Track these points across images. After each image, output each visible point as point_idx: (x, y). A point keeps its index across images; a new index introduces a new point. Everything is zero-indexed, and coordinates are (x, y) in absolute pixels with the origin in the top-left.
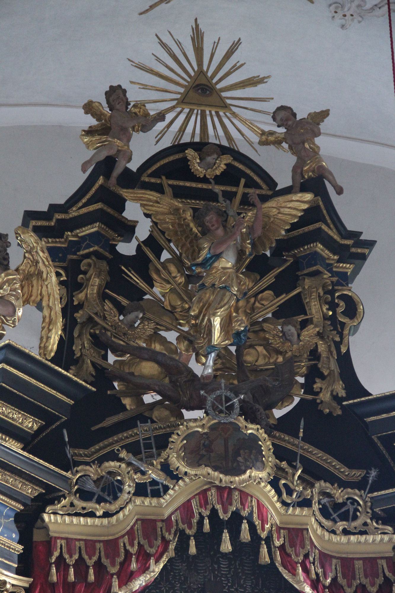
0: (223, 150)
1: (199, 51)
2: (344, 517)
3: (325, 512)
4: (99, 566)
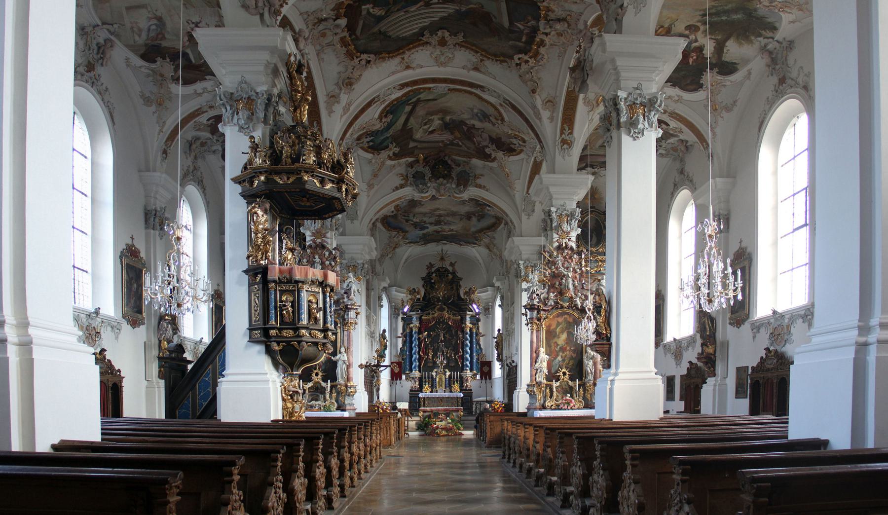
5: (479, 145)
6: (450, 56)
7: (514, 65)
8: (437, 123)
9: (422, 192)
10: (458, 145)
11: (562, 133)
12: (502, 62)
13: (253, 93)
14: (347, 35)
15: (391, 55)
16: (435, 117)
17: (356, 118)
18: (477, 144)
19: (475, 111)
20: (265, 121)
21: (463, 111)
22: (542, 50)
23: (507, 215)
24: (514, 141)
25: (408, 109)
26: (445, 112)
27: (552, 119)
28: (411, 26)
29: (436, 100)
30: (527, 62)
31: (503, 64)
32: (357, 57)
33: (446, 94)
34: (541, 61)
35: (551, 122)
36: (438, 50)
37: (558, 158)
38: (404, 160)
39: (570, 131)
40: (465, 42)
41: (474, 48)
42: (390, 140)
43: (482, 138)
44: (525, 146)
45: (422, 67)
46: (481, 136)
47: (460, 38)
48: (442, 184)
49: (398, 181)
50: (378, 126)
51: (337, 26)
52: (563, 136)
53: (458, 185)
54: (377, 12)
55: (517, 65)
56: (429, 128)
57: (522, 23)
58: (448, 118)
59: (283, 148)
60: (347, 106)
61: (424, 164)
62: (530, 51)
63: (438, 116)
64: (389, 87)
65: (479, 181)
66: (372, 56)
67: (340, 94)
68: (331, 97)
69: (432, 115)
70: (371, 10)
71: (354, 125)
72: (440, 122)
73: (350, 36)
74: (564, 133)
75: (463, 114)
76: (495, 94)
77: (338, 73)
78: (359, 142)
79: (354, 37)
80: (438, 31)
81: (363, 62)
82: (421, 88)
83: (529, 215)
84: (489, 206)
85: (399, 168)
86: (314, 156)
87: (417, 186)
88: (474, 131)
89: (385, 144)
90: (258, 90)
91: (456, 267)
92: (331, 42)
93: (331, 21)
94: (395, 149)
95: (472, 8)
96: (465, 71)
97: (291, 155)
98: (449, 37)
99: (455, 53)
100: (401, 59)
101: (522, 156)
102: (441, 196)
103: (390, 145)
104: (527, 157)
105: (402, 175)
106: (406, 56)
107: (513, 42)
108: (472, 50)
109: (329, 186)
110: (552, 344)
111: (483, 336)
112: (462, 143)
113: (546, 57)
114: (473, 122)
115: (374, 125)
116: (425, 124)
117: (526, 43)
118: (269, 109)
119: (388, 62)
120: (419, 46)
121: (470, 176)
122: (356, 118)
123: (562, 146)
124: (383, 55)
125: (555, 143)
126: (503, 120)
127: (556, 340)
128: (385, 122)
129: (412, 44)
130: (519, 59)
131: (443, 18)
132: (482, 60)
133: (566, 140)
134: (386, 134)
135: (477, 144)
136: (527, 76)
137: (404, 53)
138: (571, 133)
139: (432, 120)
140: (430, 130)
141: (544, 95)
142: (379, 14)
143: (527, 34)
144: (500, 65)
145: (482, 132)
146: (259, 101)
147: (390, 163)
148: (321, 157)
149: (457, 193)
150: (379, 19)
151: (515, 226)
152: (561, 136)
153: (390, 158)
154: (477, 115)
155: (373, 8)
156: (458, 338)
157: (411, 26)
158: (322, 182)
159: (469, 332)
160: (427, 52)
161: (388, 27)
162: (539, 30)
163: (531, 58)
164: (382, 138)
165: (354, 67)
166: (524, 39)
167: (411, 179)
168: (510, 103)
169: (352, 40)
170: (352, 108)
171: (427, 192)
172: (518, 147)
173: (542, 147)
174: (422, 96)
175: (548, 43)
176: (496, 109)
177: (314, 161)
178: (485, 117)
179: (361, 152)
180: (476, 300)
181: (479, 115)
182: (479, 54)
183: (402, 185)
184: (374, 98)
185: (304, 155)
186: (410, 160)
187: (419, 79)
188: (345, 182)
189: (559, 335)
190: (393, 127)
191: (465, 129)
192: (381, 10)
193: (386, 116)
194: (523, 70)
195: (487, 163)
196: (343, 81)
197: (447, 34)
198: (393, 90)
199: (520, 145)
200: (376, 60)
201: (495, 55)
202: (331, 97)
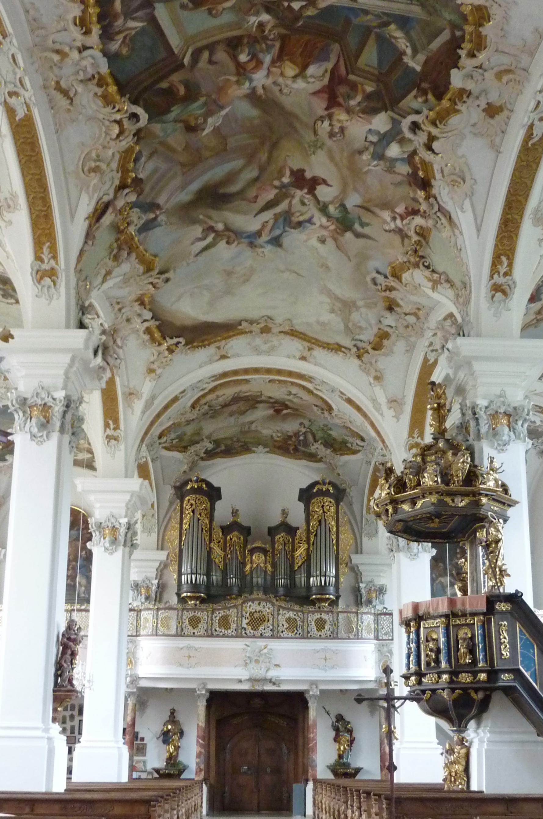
57: (133, 32)
70: (409, 51)
79: (458, 33)
143: (116, 17)
155: (404, 53)
192: (396, 38)
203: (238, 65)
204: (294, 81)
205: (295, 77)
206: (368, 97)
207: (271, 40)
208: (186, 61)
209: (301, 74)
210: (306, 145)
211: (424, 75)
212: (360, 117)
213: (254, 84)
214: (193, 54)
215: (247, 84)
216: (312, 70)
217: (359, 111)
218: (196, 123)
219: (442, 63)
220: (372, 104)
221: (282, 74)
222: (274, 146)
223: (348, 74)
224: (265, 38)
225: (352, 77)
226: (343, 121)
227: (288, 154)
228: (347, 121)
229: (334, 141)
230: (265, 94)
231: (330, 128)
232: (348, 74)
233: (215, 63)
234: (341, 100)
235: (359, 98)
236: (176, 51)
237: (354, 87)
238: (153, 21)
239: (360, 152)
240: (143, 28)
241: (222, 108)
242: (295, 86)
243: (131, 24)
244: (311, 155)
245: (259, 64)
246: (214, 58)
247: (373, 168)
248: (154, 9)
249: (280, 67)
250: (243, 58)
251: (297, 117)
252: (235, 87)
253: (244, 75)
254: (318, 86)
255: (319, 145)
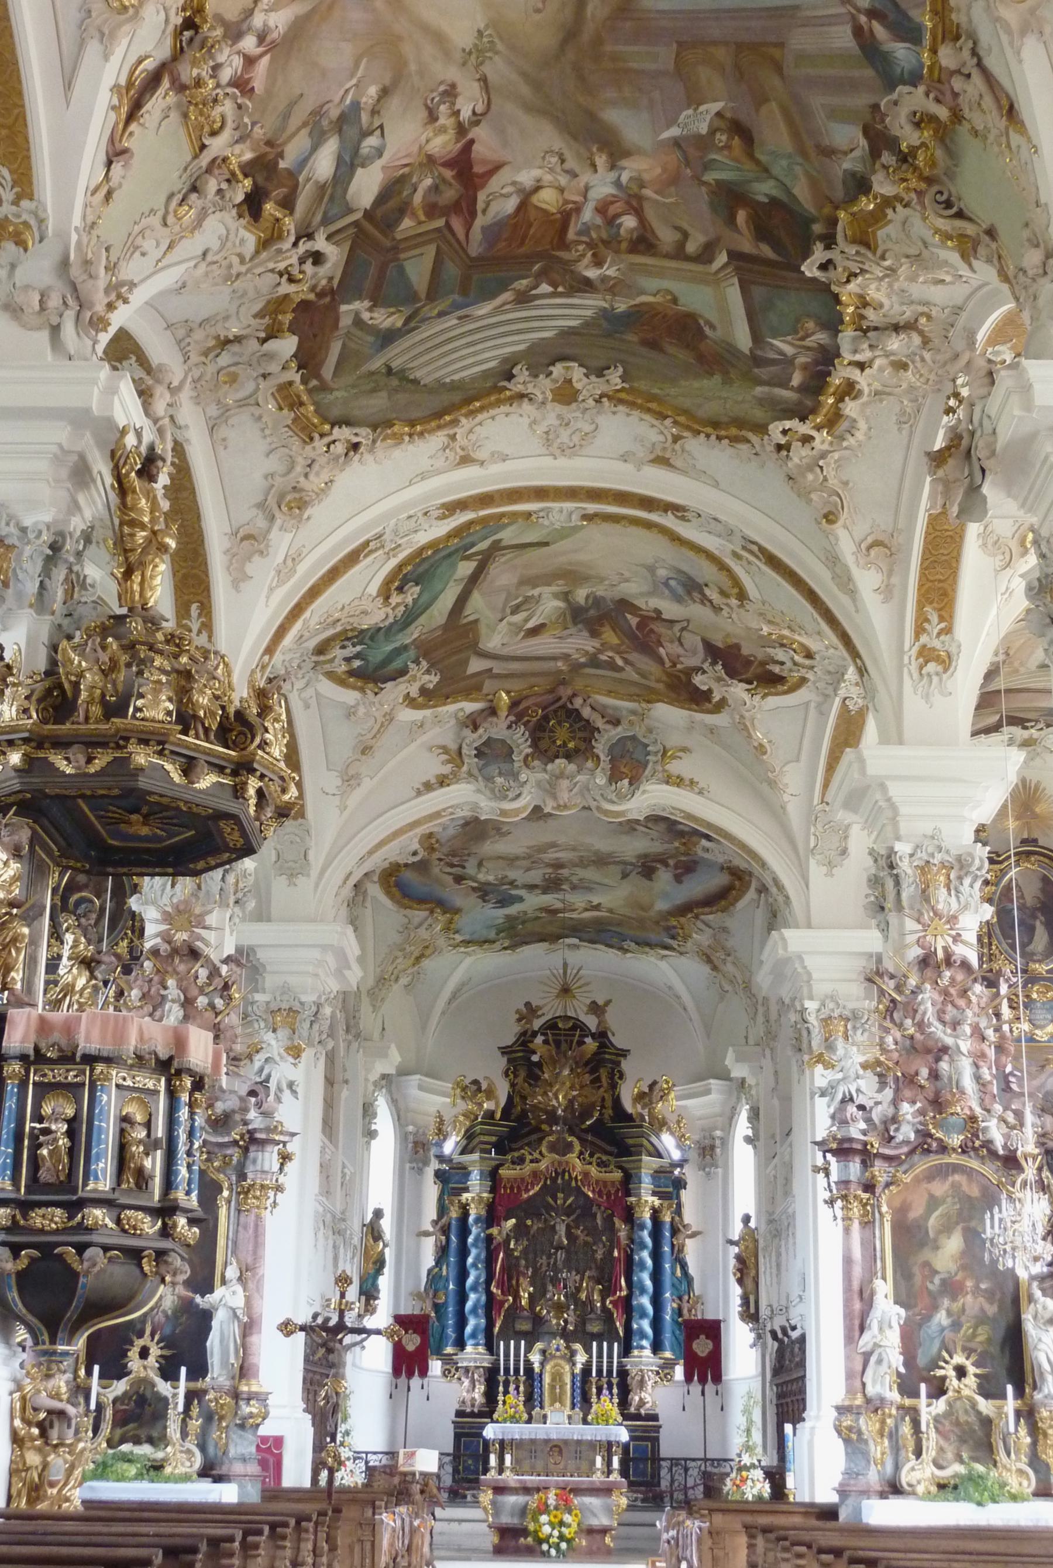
0: (571, 1018)
1: (565, 973)
2: (606, 1166)
3: (598, 1165)
4: (519, 1188)
5: (674, 665)
6: (588, 428)
7: (770, 448)
8: (549, 606)
9: (505, 798)
10: (612, 666)
11: (919, 630)
12: (734, 440)
13: (12, 529)
14: (297, 378)
15: (419, 428)
16: (546, 591)
17: (314, 593)
18: (668, 664)
19: (662, 573)
20: (41, 601)
21: (627, 574)
22: (850, 408)
23: (763, 864)
24: (780, 654)
25: (466, 568)
26: (572, 576)
27: (887, 592)
28: (475, 354)
29: (546, 544)
30: (807, 439)
31: (740, 446)
32: (322, 436)
33: (576, 529)
34: (848, 436)
35: (885, 601)
36: (553, 415)
37: (912, 701)
38: (451, 708)
39: (943, 625)
40: (631, 391)
41: (653, 405)
42: (412, 653)
43: (681, 644)
44: (812, 668)
45: (505, 458)
46: (679, 640)
47: (615, 378)
48: (561, 775)
49: (435, 766)
50: (377, 615)
51: (269, 356)
52: (924, 639)
53: (614, 777)
54: (384, 319)
55: (779, 447)
56: (526, 620)
57: (789, 338)
58: (581, 595)
59: (81, 675)
60: (289, 562)
61: (512, 718)
62: (814, 411)
63: (554, 589)
64: (411, 512)
65: (675, 767)
66: (364, 431)
67: (268, 531)
68: (242, 540)
69: (535, 587)
70: (366, 316)
71: (307, 614)
72: (561, 604)
73: (304, 381)
74: (924, 630)
75: (627, 581)
76: (719, 528)
77: (266, 477)
78: (322, 658)
80: (553, 364)
81: (339, 448)
82: (503, 515)
83: (830, 865)
84: (708, 838)
85: (437, 730)
86: (170, 700)
87: (489, 779)
88: (659, 628)
89: (397, 664)
90: (27, 522)
91: (612, 1018)
92: (250, 396)
93: (253, 344)
94: (427, 677)
95: (642, 304)
96: (629, 467)
97: (103, 695)
98: (585, 380)
99: (601, 420)
100: (446, 440)
101: (803, 695)
102: (558, 807)
103: (411, 666)
104: (820, 699)
105: (445, 750)
106: (460, 432)
107: (766, 389)
108: (649, 410)
109: (207, 781)
110: (916, 1270)
111: (694, 1235)
112: (626, 661)
113: (862, 425)
114: (654, 603)
115: (365, 613)
116: (515, 610)
117: (802, 389)
118: (55, 571)
119: (411, 447)
120: (498, 403)
121: (648, 754)
122: (314, 593)
123: (921, 668)
124: (396, 429)
125: (901, 659)
126: (742, 596)
127: (926, 1254)
128: (398, 605)
129: (477, 400)
130: (785, 432)
131: (567, 333)
132: (676, 439)
133: (934, 649)
134: (400, 636)
135: (668, 664)
136: (810, 477)
137: (455, 422)
138: (948, 631)
139: (538, 599)
140: (530, 625)
141: (861, 529)
142: (387, 323)
143: (805, 367)
144: (730, 451)
145: (683, 629)
146: (28, 550)
147: (408, 715)
148: (190, 700)
149: (613, 802)
150: (388, 338)
151: (787, 897)
152: (917, 636)
153: (411, 702)
154: (666, 584)
155: (370, 309)
156: (614, 1242)
157: (475, 354)
158: (189, 768)
159: (649, 1223)
160: (521, 420)
161: (415, 357)
162: (839, 356)
163: (818, 428)
164: (389, 648)
165: (313, 461)
166: (796, 380)
167: (471, 761)
168: (762, 549)
169: (310, 392)
170: (302, 568)
171: (519, 795)
172: (791, 670)
173: (862, 671)
174: (508, 535)
175: (866, 390)
176: (723, 567)
177: (169, 713)
178: (692, 588)
179: (328, 688)
180: (672, 1119)
181: (672, 583)
182: (668, 422)
183: (445, 776)
184: (367, 543)
185: (141, 696)
186: (470, 707)
187: (498, 491)
188: (255, 770)
189: (935, 1240)
190: (422, 620)
191: (633, 621)
192: (393, 314)
193: (400, 589)
194: (796, 460)
195: (699, 716)
196: (281, 497)
197: (577, 373)
198: (422, 519)
199: (795, 664)
200: (374, 441)
201: (716, 425)
202: (242, 540)
203: (639, 213)
204: (538, 181)
205: (537, 189)
206: (403, 210)
207: (583, 242)
208: (722, 258)
209: (527, 196)
210: (500, 46)
211: (332, 309)
212: (406, 165)
213: (612, 176)
214: (710, 261)
215: (624, 179)
216: (510, 205)
217: (409, 175)
218: (730, 138)
219: (315, 336)
220: (392, 204)
221: (562, 190)
222: (570, 34)
223: (447, 224)
224: (591, 245)
225: (440, 223)
226: (436, 135)
227: (537, 17)
228: (428, 141)
229: (441, 83)
230: (592, 154)
231: (457, 107)
232: (447, 224)
233: (677, 228)
234: (448, 174)
235: (418, 199)
236: (736, 280)
237: (432, 210)
238: (757, 337)
239: (385, 93)
240: (774, 338)
241: (676, 143)
242: (536, 173)
243: (789, 350)
244: (487, 26)
245: (602, 209)
246: (678, 236)
247: (347, 86)
248: (751, 350)
249: (566, 202)
250: (629, 222)
251: (529, 108)
252: (646, 177)
253: (630, 195)
254: (495, 184)
255: (473, 57)
